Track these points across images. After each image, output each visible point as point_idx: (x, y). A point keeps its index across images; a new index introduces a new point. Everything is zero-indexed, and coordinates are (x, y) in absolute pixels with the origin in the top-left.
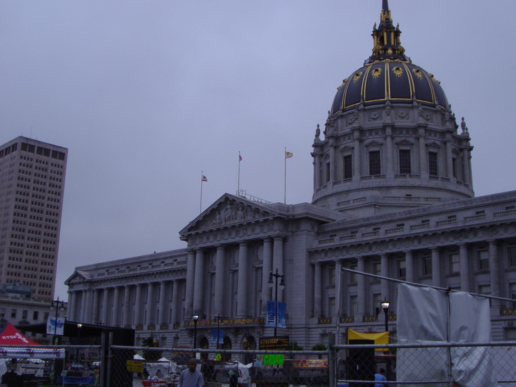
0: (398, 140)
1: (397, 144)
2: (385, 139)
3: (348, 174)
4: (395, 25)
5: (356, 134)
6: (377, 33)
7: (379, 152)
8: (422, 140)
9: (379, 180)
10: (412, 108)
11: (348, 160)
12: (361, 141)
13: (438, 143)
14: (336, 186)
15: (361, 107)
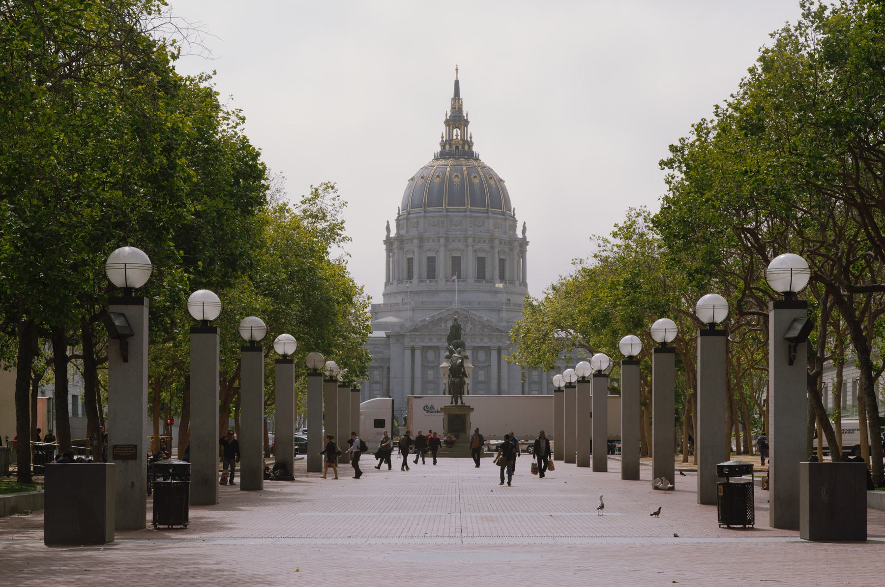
0: (476, 247)
1: (475, 251)
2: (467, 247)
3: (431, 274)
4: (465, 114)
5: (442, 241)
6: (447, 123)
7: (460, 257)
8: (496, 250)
9: (463, 284)
10: (488, 217)
11: (431, 261)
12: (446, 246)
13: (506, 249)
14: (422, 284)
15: (444, 213)
